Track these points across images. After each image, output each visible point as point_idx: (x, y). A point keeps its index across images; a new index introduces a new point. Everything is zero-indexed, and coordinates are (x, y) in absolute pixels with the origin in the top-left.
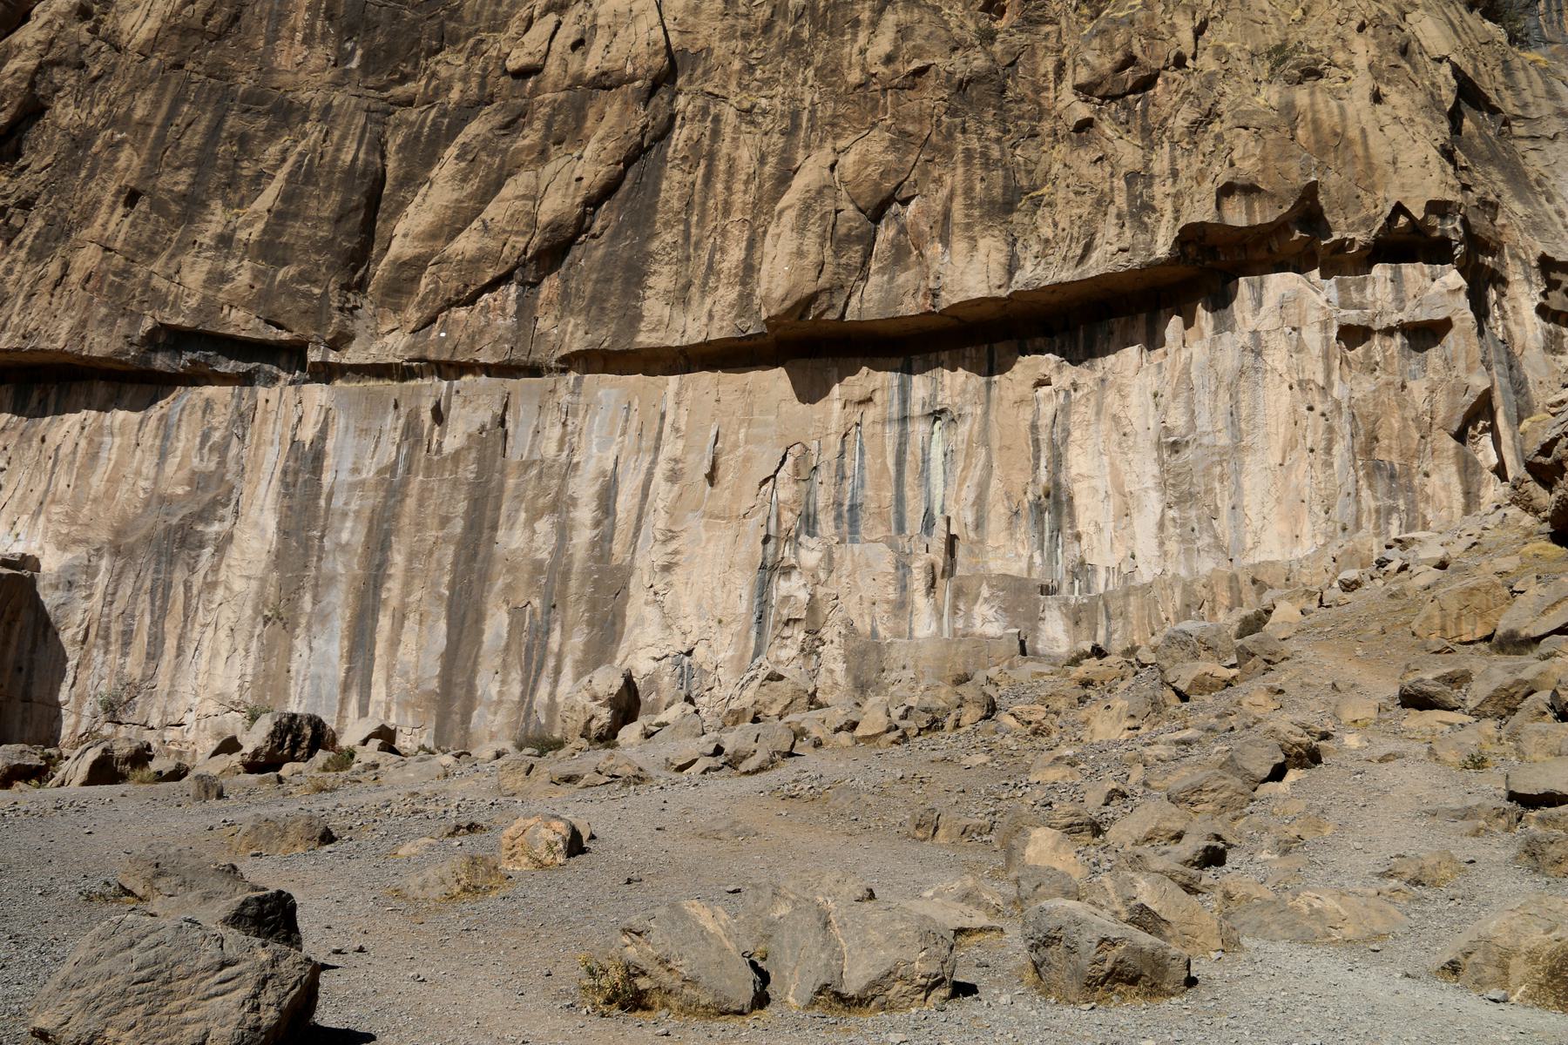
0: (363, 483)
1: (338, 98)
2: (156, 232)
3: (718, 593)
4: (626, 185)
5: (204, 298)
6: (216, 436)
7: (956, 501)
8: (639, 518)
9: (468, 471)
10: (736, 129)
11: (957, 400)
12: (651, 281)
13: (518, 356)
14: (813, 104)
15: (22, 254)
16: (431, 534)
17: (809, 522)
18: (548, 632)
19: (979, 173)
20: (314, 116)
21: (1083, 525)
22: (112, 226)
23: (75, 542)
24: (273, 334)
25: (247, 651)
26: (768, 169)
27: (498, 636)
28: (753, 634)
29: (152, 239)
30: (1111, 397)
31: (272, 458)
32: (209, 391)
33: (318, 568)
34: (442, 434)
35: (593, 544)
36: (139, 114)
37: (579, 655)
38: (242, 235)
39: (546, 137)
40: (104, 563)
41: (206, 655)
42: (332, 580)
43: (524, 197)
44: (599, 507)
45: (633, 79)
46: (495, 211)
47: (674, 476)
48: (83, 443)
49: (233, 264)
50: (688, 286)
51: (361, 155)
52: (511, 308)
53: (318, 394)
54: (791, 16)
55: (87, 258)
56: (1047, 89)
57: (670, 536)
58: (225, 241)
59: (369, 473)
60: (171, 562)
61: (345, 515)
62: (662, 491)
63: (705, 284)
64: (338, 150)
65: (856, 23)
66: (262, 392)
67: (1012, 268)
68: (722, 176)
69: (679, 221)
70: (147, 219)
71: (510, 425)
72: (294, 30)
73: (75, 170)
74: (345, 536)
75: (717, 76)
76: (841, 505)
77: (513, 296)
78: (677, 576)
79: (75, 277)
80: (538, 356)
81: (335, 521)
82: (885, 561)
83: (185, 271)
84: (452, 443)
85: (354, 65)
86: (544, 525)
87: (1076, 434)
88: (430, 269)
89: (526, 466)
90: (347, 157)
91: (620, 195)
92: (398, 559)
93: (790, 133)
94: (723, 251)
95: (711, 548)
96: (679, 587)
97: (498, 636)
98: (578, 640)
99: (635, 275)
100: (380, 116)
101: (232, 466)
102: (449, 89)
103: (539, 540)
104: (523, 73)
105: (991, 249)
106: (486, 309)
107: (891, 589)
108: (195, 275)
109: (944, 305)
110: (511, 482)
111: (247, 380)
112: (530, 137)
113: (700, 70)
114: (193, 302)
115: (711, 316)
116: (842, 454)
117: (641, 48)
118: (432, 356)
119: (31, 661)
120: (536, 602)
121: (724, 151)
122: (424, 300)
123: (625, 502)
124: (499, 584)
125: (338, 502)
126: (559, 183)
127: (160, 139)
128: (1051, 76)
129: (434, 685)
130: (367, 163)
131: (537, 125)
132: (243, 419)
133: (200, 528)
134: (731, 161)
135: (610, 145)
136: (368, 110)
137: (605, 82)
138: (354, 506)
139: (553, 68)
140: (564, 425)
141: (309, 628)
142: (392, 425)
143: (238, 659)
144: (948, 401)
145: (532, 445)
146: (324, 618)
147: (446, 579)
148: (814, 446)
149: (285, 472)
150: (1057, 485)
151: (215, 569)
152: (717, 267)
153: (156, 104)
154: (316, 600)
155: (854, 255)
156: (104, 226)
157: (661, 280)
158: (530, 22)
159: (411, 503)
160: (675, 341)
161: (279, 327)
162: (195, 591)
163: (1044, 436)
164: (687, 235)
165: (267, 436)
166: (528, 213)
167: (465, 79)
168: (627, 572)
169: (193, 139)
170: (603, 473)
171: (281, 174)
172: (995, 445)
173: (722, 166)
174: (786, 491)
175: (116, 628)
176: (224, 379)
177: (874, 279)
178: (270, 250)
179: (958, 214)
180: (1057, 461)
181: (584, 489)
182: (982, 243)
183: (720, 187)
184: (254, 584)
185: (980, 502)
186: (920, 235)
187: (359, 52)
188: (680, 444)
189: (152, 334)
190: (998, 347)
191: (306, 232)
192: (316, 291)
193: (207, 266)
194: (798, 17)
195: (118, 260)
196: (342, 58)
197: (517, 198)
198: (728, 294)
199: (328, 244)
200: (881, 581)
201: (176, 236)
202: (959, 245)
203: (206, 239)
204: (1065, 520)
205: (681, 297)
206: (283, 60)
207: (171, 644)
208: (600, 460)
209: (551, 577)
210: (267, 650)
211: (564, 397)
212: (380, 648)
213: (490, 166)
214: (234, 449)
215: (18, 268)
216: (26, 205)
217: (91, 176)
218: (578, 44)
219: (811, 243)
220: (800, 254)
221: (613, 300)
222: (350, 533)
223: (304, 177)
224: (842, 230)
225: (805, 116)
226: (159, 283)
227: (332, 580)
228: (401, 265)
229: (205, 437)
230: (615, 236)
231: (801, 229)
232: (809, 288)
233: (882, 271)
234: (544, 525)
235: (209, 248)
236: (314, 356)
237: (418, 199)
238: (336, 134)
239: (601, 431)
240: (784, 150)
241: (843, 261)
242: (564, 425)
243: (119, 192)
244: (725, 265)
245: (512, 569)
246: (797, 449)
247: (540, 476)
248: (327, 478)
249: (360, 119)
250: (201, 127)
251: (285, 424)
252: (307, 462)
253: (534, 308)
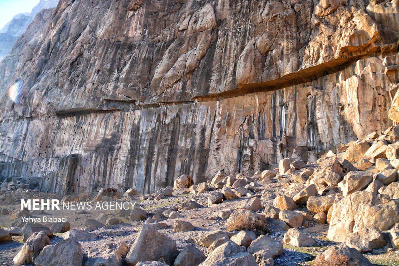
0: (148, 133)
1: (142, 43)
2: (103, 78)
3: (230, 154)
4: (207, 55)
5: (113, 92)
6: (117, 124)
7: (288, 127)
8: (211, 137)
9: (171, 128)
10: (232, 38)
11: (288, 100)
12: (212, 78)
13: (182, 100)
14: (250, 29)
15: (77, 87)
16: (163, 144)
17: (251, 136)
18: (190, 166)
19: (290, 41)
20: (137, 47)
21: (320, 131)
22: (94, 78)
23: (88, 150)
24: (128, 99)
25: (124, 174)
26: (239, 46)
27: (179, 168)
28: (238, 165)
29: (102, 80)
30: (326, 96)
31: (129, 127)
32: (115, 114)
33: (139, 153)
34: (165, 119)
35: (200, 144)
36: (100, 52)
37: (197, 172)
38: (121, 77)
39: (188, 45)
40: (94, 155)
41: (115, 175)
42: (142, 156)
43: (183, 60)
44: (201, 135)
45: (208, 28)
46: (176, 65)
47: (219, 126)
48: (89, 128)
49: (119, 84)
50: (220, 78)
51: (147, 55)
52: (180, 88)
53: (138, 112)
54: (245, 7)
55: (89, 85)
56: (308, 16)
57: (218, 141)
58: (117, 79)
59: (150, 130)
60: (108, 154)
61: (144, 140)
62: (216, 130)
63: (225, 77)
64: (142, 54)
65: (260, 7)
66: (126, 113)
67: (299, 64)
68: (228, 50)
69: (219, 62)
70: (101, 76)
71: (181, 117)
72: (132, 28)
73: (87, 67)
74: (144, 146)
75: (228, 25)
76: (259, 130)
77: (181, 85)
78: (220, 151)
79: (86, 91)
80: (187, 99)
81: (142, 142)
82: (270, 144)
83: (109, 86)
84: (167, 122)
85: (146, 34)
86: (188, 140)
87: (318, 107)
88: (163, 80)
89: (184, 126)
90: (143, 56)
91: (205, 58)
92: (156, 150)
93: (244, 37)
94: (229, 68)
95: (228, 143)
96: (221, 154)
97: (179, 168)
98: (197, 167)
99: (208, 76)
100: (152, 45)
101: (120, 130)
102: (167, 36)
103: (188, 143)
104: (183, 30)
105: (293, 60)
106: (175, 89)
107: (272, 151)
108: (111, 88)
109: (281, 76)
110: (181, 130)
111: (123, 110)
112: (185, 46)
113: (224, 24)
114: (111, 93)
115: (226, 85)
116: (259, 117)
117: (209, 20)
118: (163, 101)
119: (80, 178)
120: (187, 159)
121: (229, 43)
122: (161, 88)
123: (207, 133)
124: (179, 154)
125: (143, 137)
126: (190, 57)
127: (104, 58)
128: (309, 13)
129: (164, 180)
130: (148, 57)
131: (186, 42)
132: (122, 119)
133: (114, 146)
134: (230, 46)
135: (202, 45)
136: (149, 44)
137: (201, 30)
138: (146, 138)
139: (189, 29)
140: (193, 115)
141: (137, 168)
142: (154, 119)
143: (122, 176)
144: (285, 101)
145: (186, 121)
146: (140, 165)
147: (167, 154)
148: (252, 116)
149: (131, 132)
150: (313, 121)
151: (117, 155)
152: (227, 73)
153: (103, 50)
154: (138, 161)
155: (260, 66)
156: (92, 78)
157: (214, 77)
158: (185, 18)
159: (159, 137)
160: (218, 92)
161: (129, 97)
162: (113, 160)
163: (309, 109)
164: (221, 65)
165: (127, 123)
166: (184, 64)
167: (170, 34)
168: (208, 150)
169: (111, 56)
170: (202, 126)
171: (129, 62)
172: (297, 112)
173: (228, 47)
174: (246, 128)
175: (96, 170)
176: (119, 110)
177: (265, 72)
178: (127, 80)
179: (285, 52)
180: (313, 115)
181: (198, 130)
182: (291, 59)
183: (228, 52)
184: (125, 158)
185: (294, 127)
186: (276, 59)
187: (147, 31)
188: (220, 118)
189: (102, 102)
190: (298, 86)
191: (135, 75)
192: (137, 88)
193: (113, 85)
194: (247, 7)
195: (95, 86)
196: (144, 32)
197: (181, 61)
198: (229, 79)
199: (140, 77)
200: (269, 149)
201: (107, 79)
202: (285, 60)
203: (113, 79)
204: (316, 130)
205: (219, 82)
206: (130, 35)
207: (108, 173)
208: (201, 123)
209: (190, 153)
210: (128, 173)
211: (193, 108)
212: (152, 172)
213: (175, 54)
214: (121, 127)
215: (76, 90)
216: (78, 76)
217: (90, 68)
218: (195, 22)
219: (248, 64)
220: (245, 67)
221: (203, 83)
222: (145, 145)
223: (135, 62)
224: (256, 60)
225: (248, 32)
226: (104, 90)
227: (142, 156)
228: (156, 80)
229: (115, 124)
230: (204, 68)
231: (245, 61)
232: (248, 75)
233: (267, 69)
234: (188, 140)
235: (114, 81)
236: (137, 103)
237: (160, 64)
238: (141, 51)
239: (201, 116)
240: (243, 41)
241: (257, 68)
242: (193, 115)
243: (96, 70)
244: (229, 72)
245: (182, 151)
246: (248, 117)
247: (187, 129)
248: (141, 132)
249: (147, 47)
250: (113, 53)
251: (131, 120)
253: (185, 88)
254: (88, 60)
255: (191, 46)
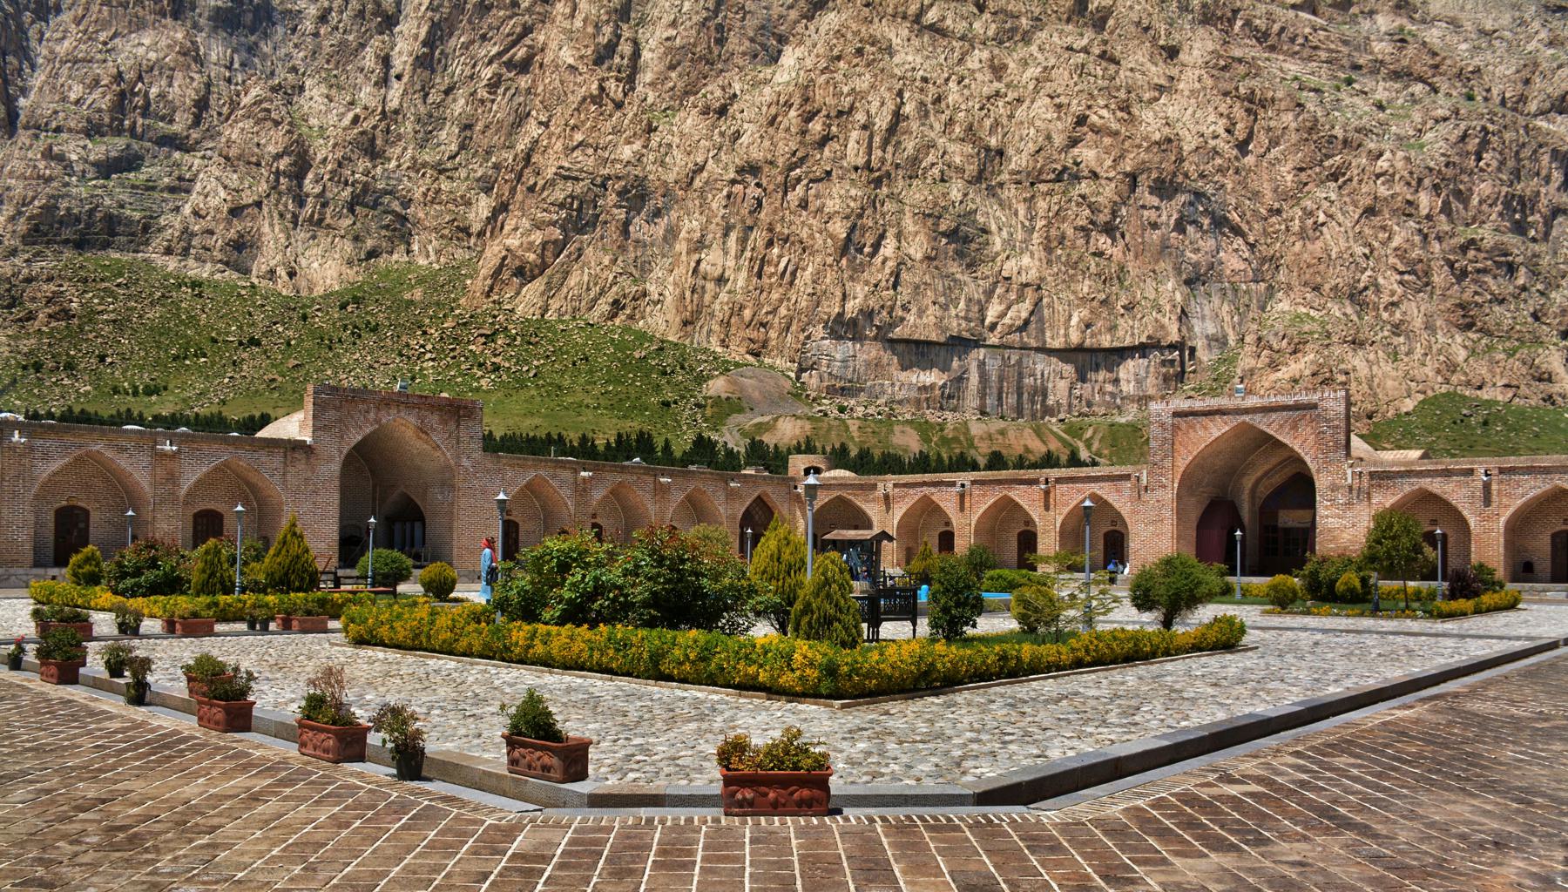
53: (982, 351)
99: (1043, 333)
126: (1024, 309)
137: (1027, 285)
157: (1048, 334)
252: (981, 364)
254: (917, 287)
255: (1021, 298)
